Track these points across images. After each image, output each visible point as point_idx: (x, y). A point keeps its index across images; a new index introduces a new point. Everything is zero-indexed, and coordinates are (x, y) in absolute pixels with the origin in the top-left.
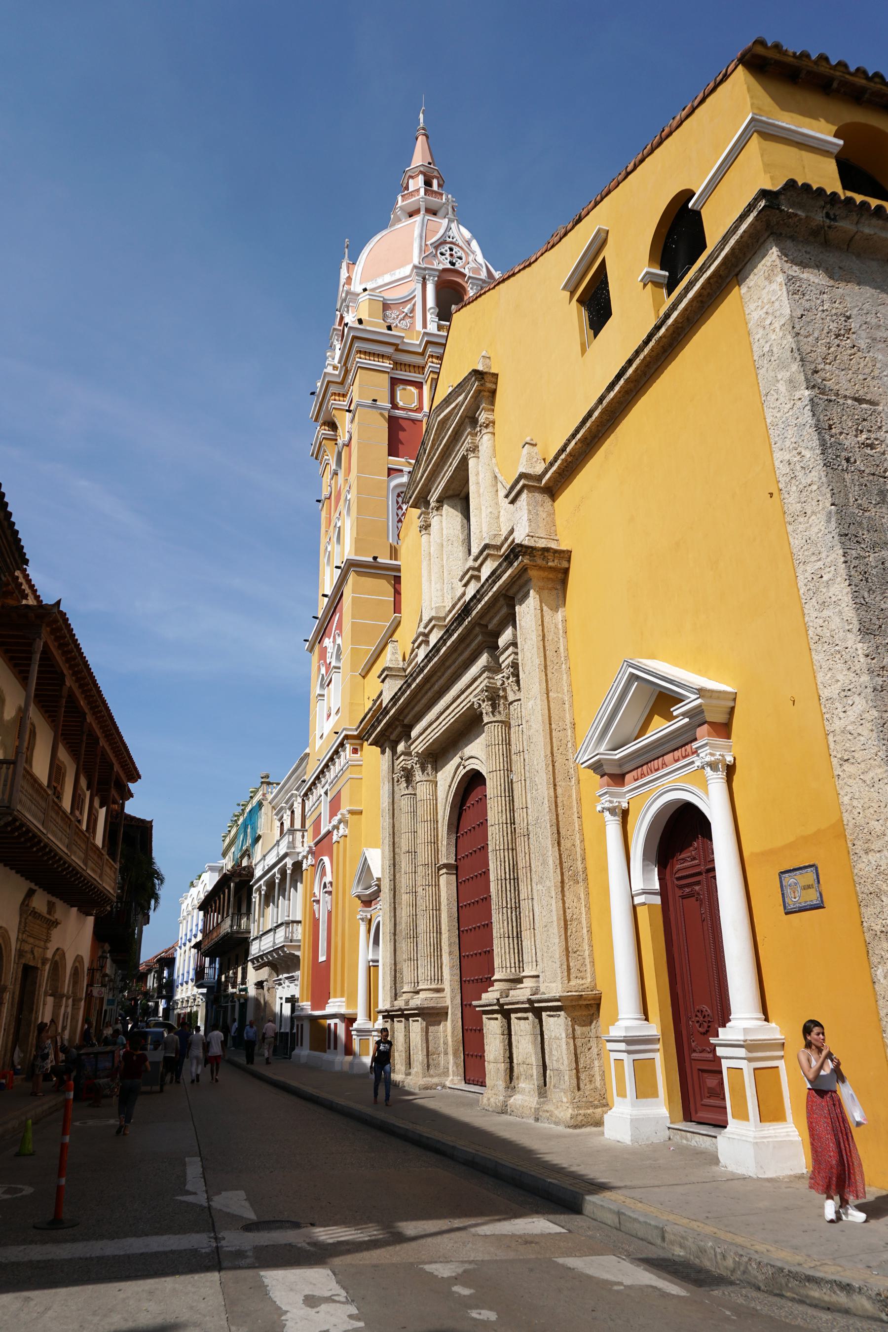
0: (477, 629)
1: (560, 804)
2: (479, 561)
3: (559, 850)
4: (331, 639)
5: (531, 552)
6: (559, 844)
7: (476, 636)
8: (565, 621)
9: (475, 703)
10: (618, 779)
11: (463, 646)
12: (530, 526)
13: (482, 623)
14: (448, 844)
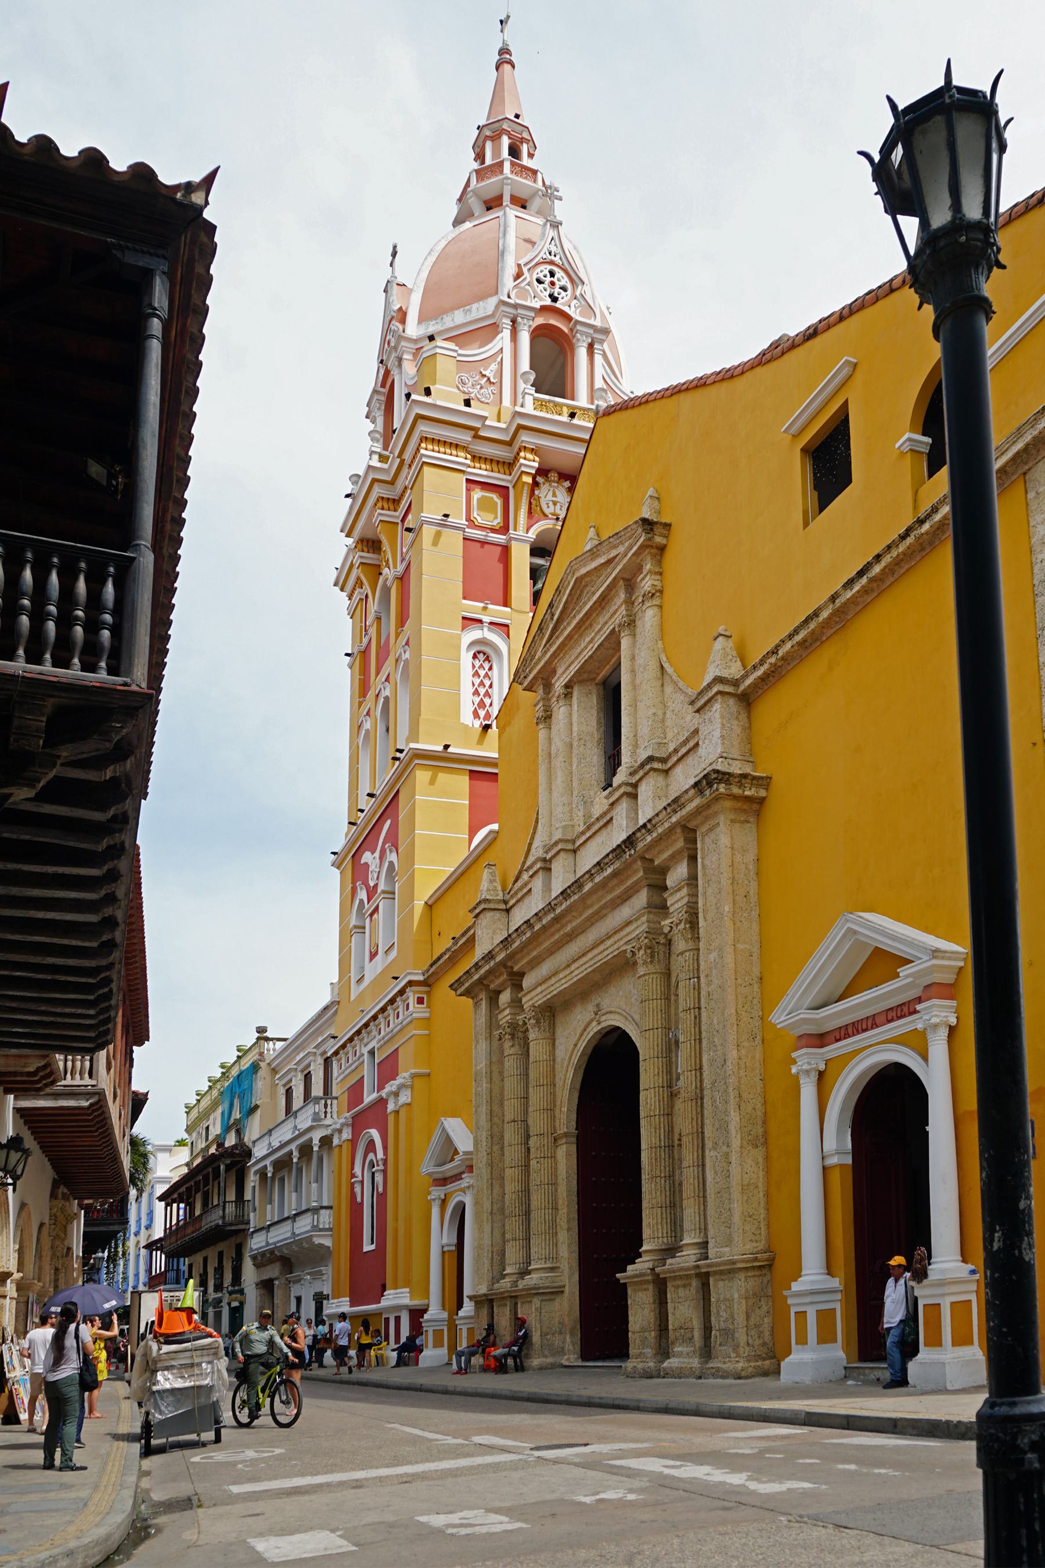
7: (635, 872)
9: (629, 951)
11: (615, 881)
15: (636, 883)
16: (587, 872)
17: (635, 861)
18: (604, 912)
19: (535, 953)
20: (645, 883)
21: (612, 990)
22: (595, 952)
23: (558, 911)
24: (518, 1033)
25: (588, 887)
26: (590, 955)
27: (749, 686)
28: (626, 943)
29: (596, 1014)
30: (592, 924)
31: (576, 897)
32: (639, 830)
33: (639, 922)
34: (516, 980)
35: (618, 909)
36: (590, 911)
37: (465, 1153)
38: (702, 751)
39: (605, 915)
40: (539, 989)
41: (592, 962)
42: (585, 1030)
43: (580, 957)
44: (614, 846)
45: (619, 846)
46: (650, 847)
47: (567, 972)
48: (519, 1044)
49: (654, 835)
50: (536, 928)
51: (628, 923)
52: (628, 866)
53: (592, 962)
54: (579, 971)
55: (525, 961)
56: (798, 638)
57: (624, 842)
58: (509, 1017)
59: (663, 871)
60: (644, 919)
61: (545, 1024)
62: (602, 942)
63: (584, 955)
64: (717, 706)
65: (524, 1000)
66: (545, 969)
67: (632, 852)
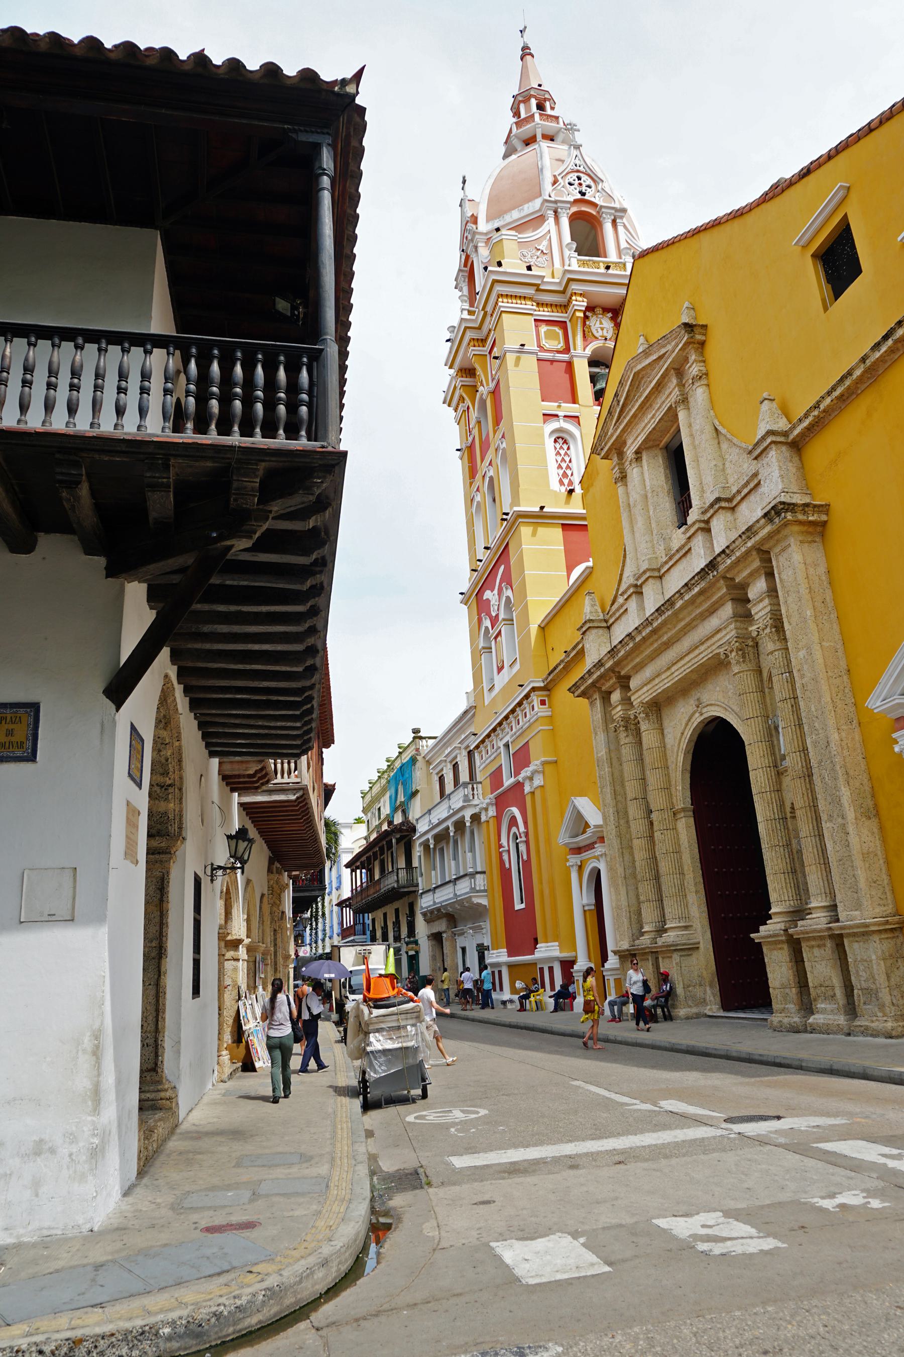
0: (722, 582)
2: (709, 515)
4: (496, 592)
5: (793, 509)
7: (719, 589)
11: (702, 598)
12: (783, 481)
13: (728, 576)
14: (683, 788)
15: (721, 598)
16: (677, 592)
17: (718, 581)
18: (695, 623)
19: (638, 660)
20: (728, 597)
21: (710, 686)
22: (691, 656)
23: (655, 624)
24: (631, 726)
25: (679, 604)
26: (687, 659)
27: (797, 435)
28: (718, 647)
29: (698, 707)
30: (685, 634)
31: (670, 613)
32: (719, 555)
33: (728, 629)
34: (624, 682)
35: (707, 620)
36: (683, 623)
37: (596, 826)
38: (763, 489)
39: (696, 626)
40: (645, 689)
41: (690, 664)
42: (689, 720)
43: (678, 661)
44: (698, 570)
45: (703, 569)
46: (730, 568)
47: (668, 673)
48: (633, 735)
49: (733, 558)
50: (637, 639)
51: (718, 631)
52: (712, 585)
53: (690, 664)
54: (679, 672)
55: (630, 667)
56: (837, 393)
57: (707, 566)
58: (621, 713)
59: (743, 587)
60: (732, 626)
61: (653, 717)
62: (697, 647)
63: (681, 659)
64: (773, 453)
65: (633, 698)
66: (648, 672)
67: (715, 573)
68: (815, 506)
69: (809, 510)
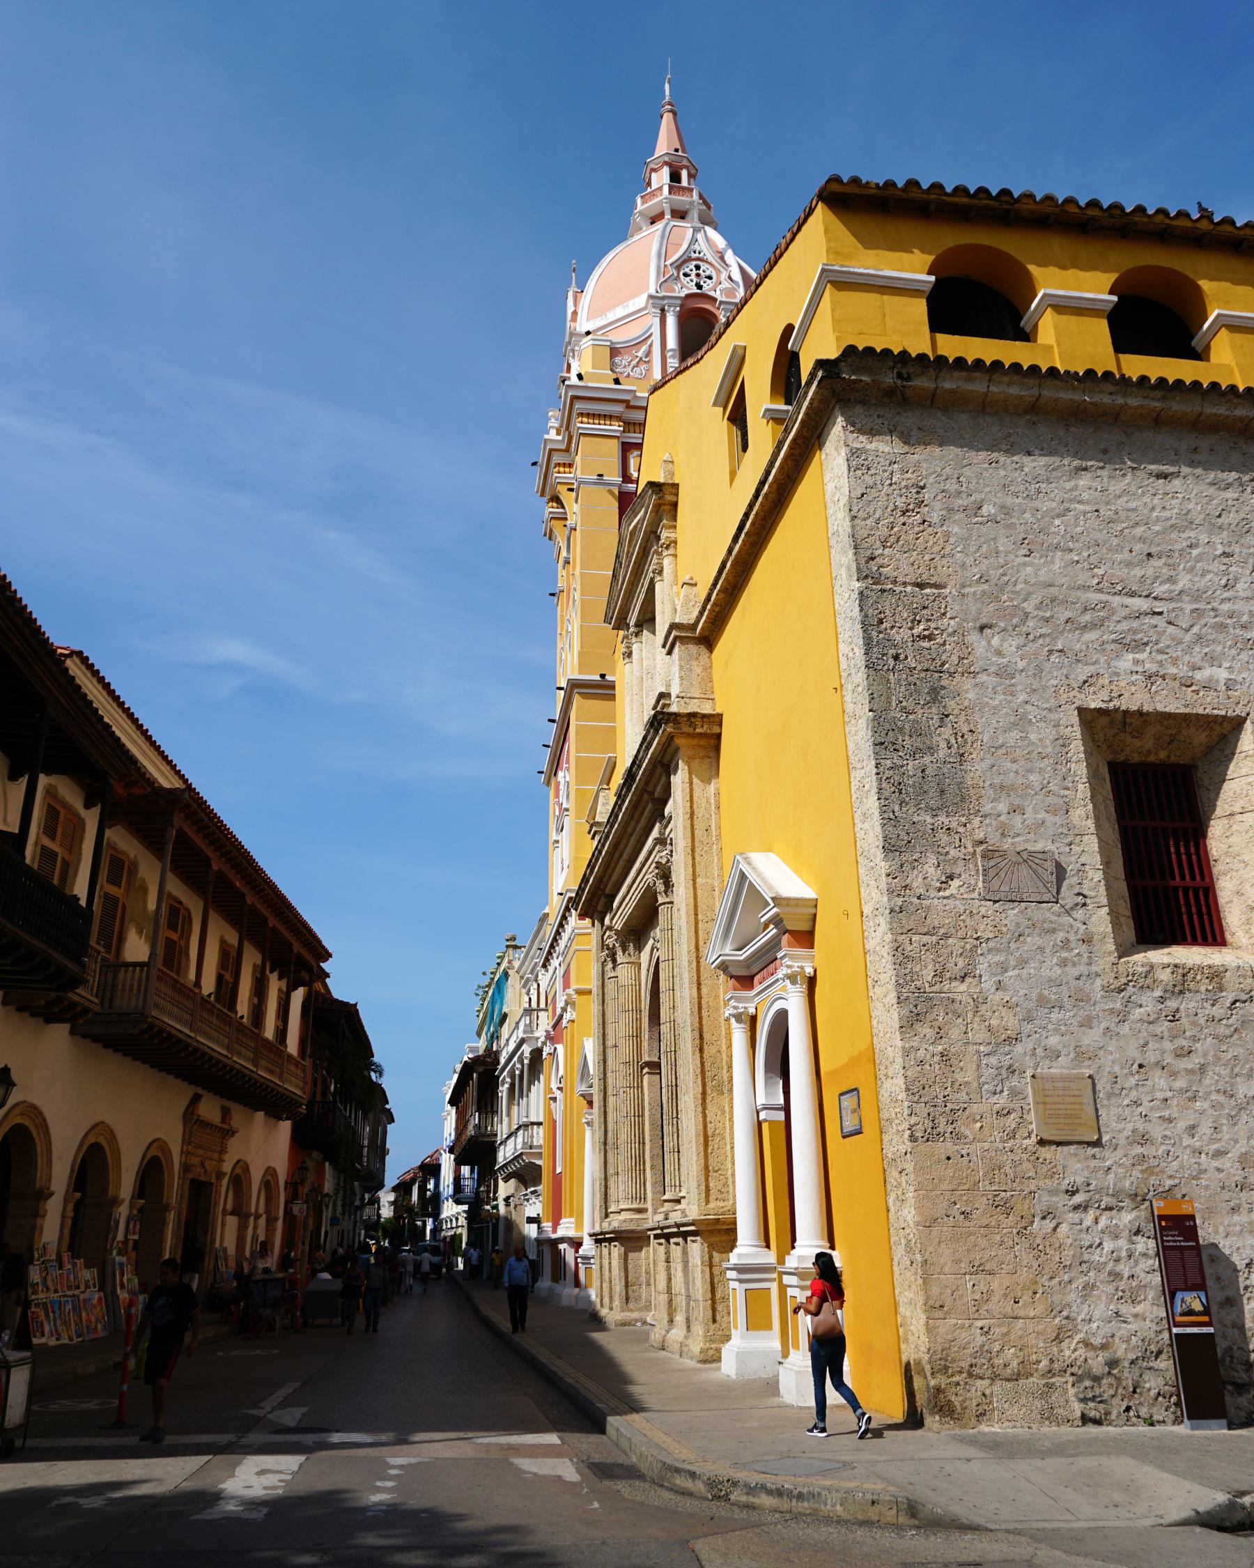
1: (704, 1006)
3: (701, 1057)
6: (701, 1050)
8: (717, 794)
10: (746, 981)
68: (704, 716)
69: (698, 722)
